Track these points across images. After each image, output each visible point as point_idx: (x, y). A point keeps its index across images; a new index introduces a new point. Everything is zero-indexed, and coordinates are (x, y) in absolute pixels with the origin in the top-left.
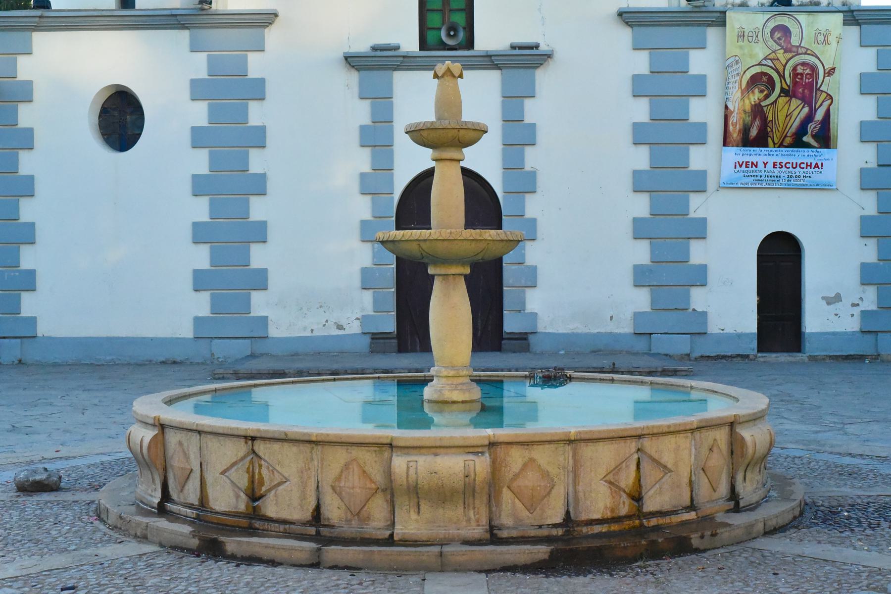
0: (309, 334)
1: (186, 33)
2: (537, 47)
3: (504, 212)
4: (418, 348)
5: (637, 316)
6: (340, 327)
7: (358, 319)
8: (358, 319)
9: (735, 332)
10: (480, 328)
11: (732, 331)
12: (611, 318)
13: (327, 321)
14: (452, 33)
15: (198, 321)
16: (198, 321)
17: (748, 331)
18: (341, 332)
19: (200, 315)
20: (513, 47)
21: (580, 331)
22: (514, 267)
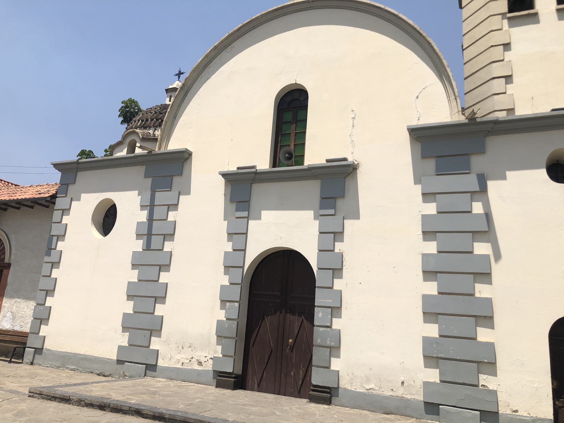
0: (179, 366)
1: (144, 167)
2: (345, 159)
3: (317, 284)
4: (256, 387)
5: (426, 384)
6: (200, 363)
7: (211, 358)
8: (211, 358)
9: (528, 415)
10: (301, 377)
11: (525, 414)
12: (403, 383)
13: (192, 358)
14: (287, 155)
15: (120, 348)
16: (120, 348)
17: (542, 416)
18: (200, 368)
19: (123, 344)
20: (328, 161)
21: (373, 391)
22: (321, 329)
